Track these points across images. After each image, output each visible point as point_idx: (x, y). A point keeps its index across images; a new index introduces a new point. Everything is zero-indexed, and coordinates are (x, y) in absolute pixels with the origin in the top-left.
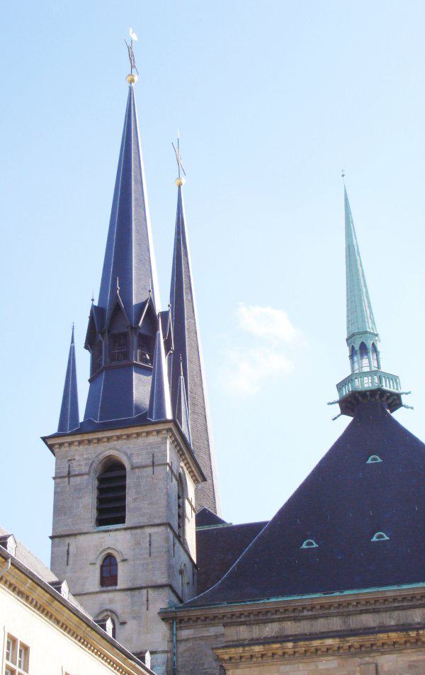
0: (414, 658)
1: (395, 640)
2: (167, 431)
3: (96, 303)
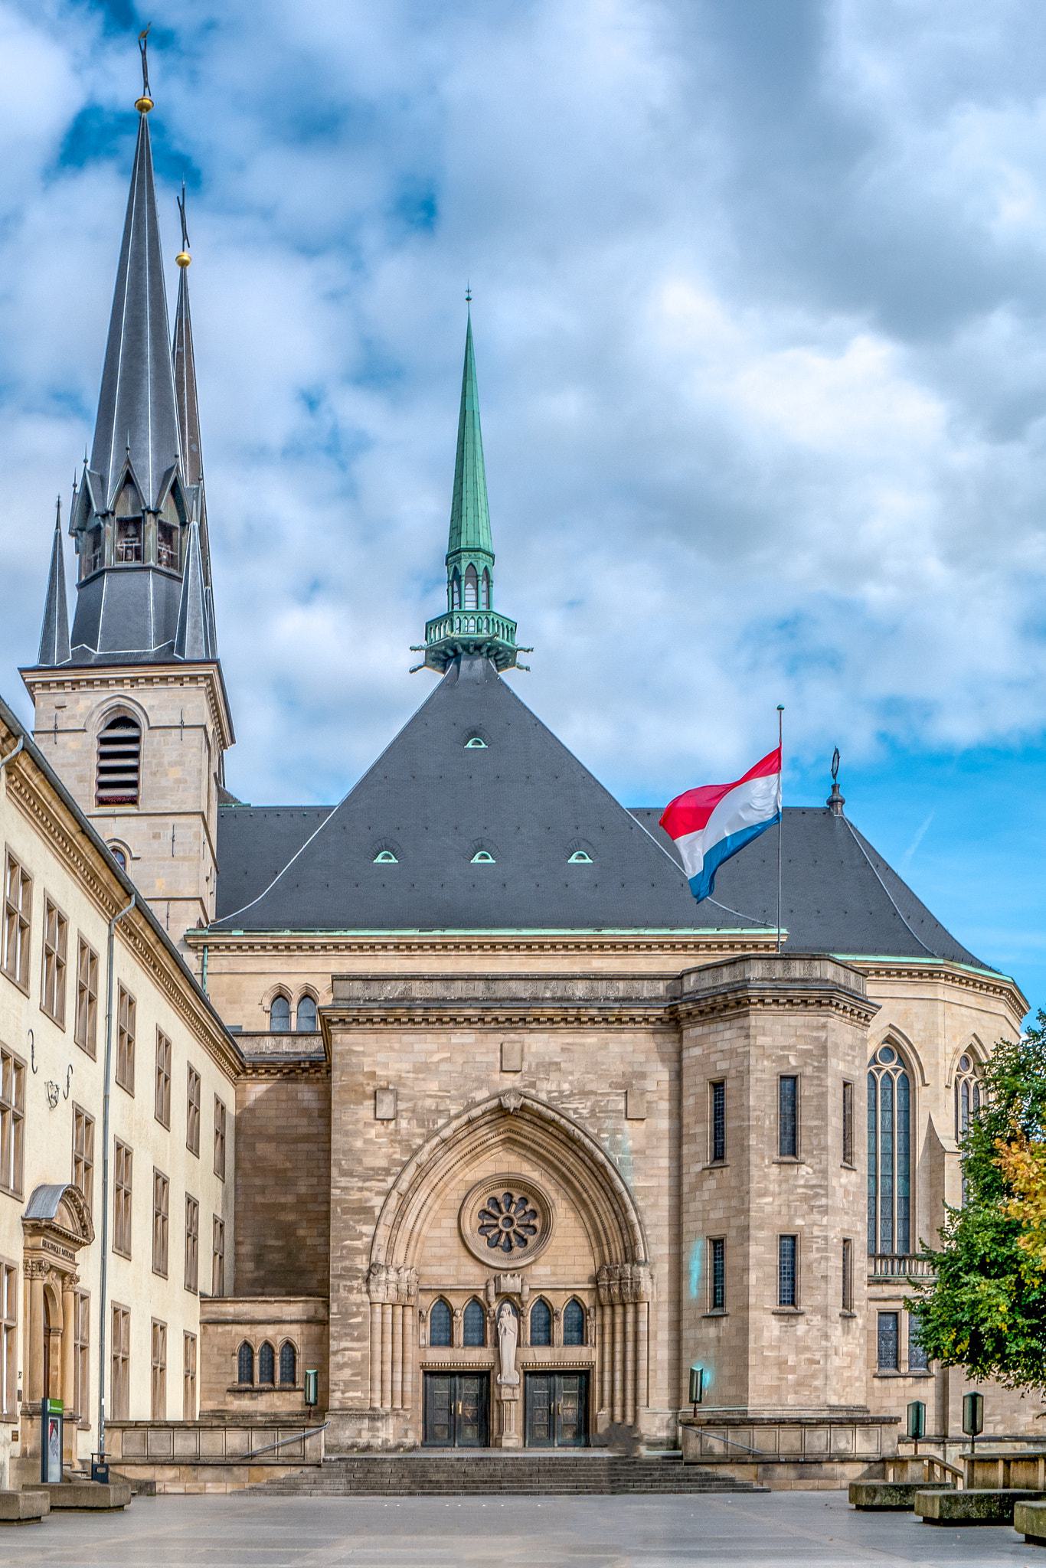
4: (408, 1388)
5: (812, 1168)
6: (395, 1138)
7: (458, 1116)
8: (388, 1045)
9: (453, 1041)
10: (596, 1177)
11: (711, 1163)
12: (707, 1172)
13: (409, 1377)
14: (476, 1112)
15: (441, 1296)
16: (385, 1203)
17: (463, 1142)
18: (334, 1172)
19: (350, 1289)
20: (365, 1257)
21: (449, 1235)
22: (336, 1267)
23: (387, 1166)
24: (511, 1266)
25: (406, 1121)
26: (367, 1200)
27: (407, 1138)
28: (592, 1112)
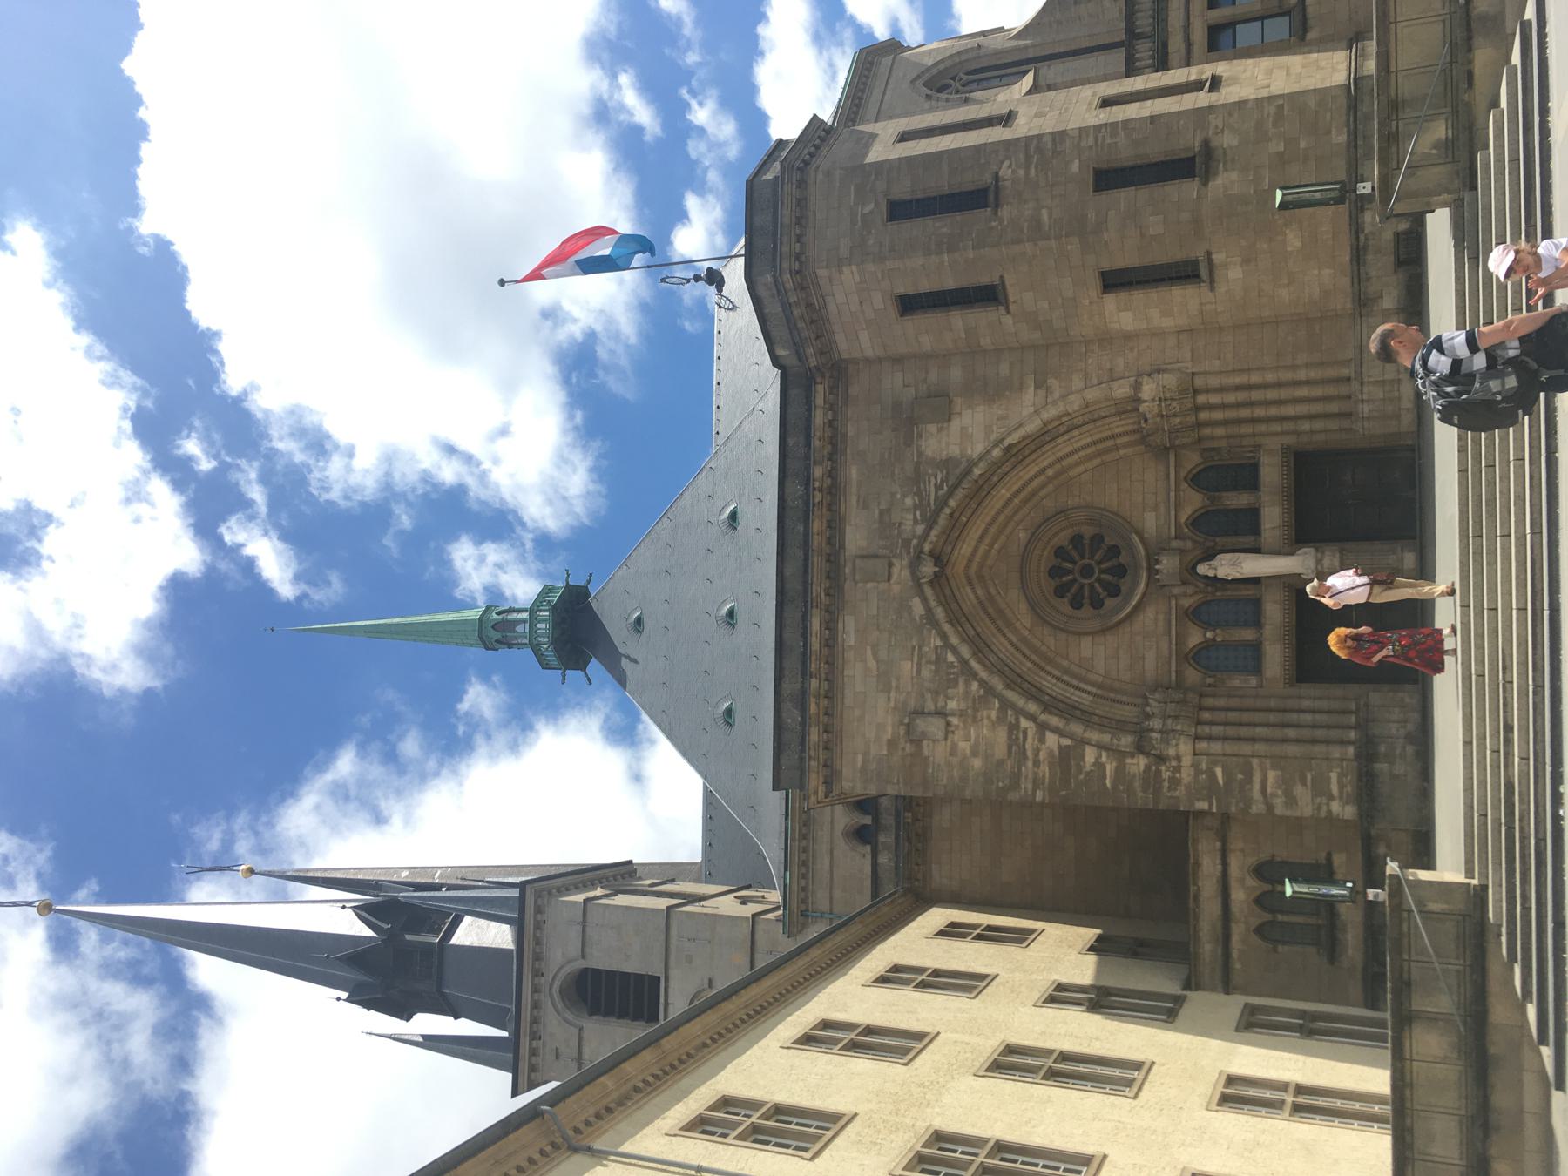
0: (854, 500)
1: (825, 525)
2: (540, 897)
3: (344, 995)
4: (1324, 704)
5: (1002, 162)
6: (970, 715)
7: (944, 636)
8: (856, 724)
9: (852, 643)
10: (1024, 458)
11: (1001, 304)
12: (1012, 307)
13: (1306, 703)
14: (940, 613)
15: (1186, 657)
16: (1056, 730)
17: (979, 630)
18: (1013, 796)
19: (1175, 782)
20: (1129, 761)
21: (1102, 648)
22: (1142, 799)
23: (1006, 728)
24: (1144, 565)
25: (949, 702)
26: (1051, 752)
27: (970, 703)
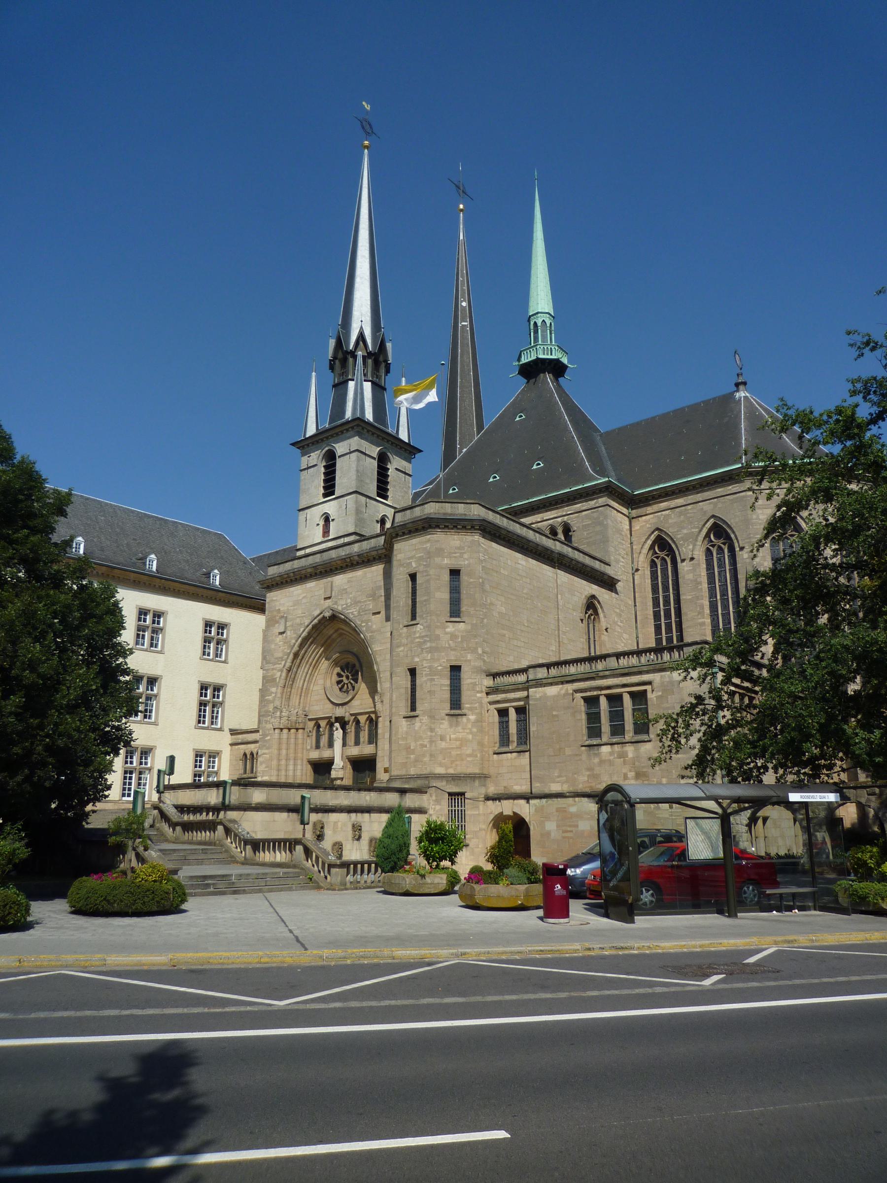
7: (308, 626)
28: (359, 612)
